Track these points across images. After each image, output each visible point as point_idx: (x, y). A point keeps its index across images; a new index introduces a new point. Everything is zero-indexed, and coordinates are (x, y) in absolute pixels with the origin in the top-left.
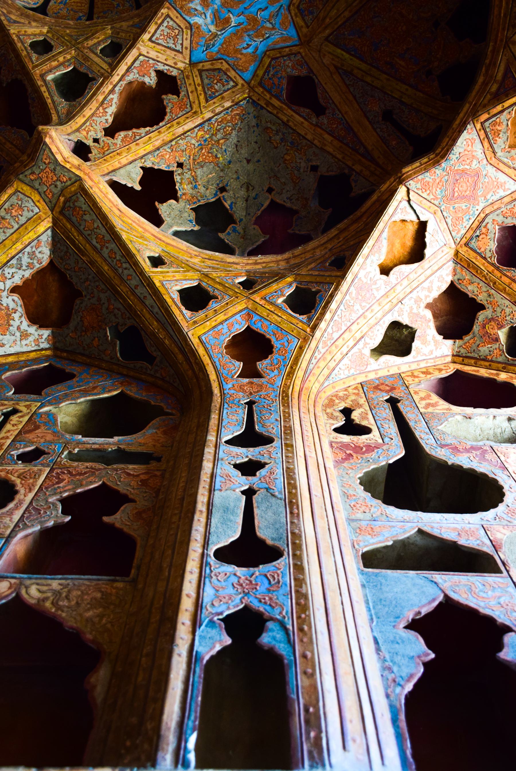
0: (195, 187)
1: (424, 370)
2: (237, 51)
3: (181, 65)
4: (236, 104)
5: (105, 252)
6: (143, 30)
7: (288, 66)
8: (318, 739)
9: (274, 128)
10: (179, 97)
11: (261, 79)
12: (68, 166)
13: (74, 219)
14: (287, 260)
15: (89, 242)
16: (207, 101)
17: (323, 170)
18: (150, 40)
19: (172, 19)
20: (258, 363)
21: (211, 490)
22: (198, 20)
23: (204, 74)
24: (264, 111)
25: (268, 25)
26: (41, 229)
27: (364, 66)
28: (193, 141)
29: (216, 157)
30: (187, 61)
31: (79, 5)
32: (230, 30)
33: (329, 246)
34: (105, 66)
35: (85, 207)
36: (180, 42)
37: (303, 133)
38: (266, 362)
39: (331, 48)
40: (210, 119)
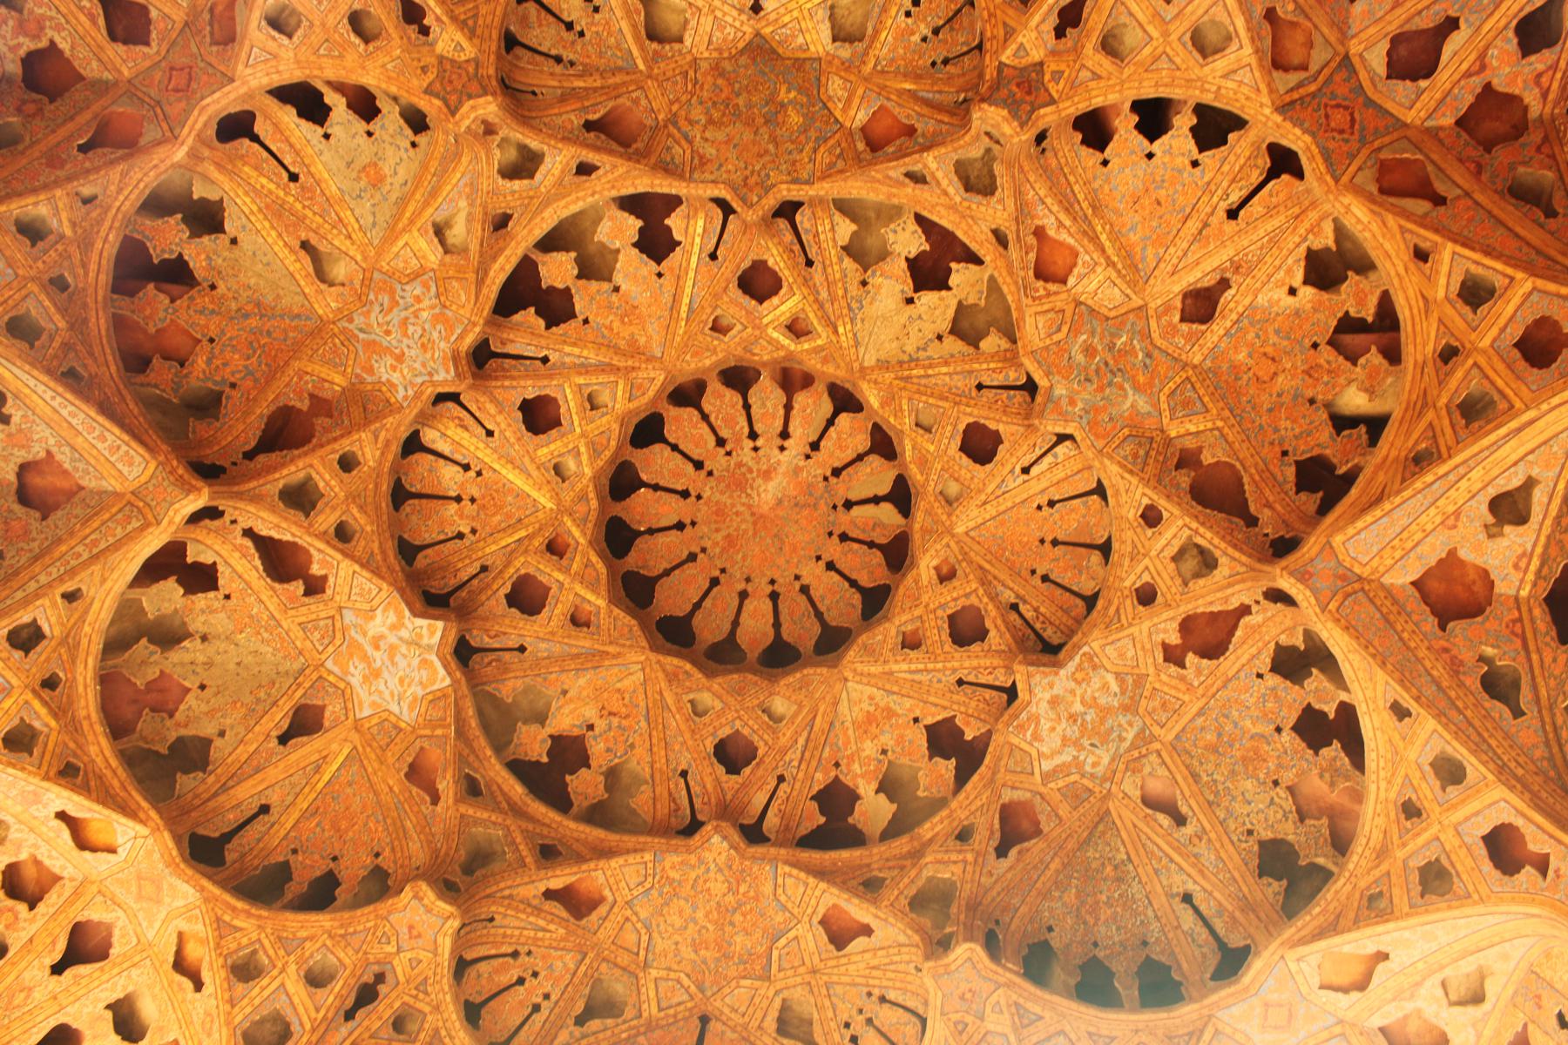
0: (203, 612)
2: (351, 656)
3: (337, 598)
5: (80, 549)
6: (362, 565)
12: (171, 513)
13: (120, 516)
14: (88, 717)
17: (218, 742)
26: (113, 482)
27: (320, 785)
32: (369, 650)
33: (99, 760)
34: (322, 529)
35: (130, 528)
39: (346, 751)
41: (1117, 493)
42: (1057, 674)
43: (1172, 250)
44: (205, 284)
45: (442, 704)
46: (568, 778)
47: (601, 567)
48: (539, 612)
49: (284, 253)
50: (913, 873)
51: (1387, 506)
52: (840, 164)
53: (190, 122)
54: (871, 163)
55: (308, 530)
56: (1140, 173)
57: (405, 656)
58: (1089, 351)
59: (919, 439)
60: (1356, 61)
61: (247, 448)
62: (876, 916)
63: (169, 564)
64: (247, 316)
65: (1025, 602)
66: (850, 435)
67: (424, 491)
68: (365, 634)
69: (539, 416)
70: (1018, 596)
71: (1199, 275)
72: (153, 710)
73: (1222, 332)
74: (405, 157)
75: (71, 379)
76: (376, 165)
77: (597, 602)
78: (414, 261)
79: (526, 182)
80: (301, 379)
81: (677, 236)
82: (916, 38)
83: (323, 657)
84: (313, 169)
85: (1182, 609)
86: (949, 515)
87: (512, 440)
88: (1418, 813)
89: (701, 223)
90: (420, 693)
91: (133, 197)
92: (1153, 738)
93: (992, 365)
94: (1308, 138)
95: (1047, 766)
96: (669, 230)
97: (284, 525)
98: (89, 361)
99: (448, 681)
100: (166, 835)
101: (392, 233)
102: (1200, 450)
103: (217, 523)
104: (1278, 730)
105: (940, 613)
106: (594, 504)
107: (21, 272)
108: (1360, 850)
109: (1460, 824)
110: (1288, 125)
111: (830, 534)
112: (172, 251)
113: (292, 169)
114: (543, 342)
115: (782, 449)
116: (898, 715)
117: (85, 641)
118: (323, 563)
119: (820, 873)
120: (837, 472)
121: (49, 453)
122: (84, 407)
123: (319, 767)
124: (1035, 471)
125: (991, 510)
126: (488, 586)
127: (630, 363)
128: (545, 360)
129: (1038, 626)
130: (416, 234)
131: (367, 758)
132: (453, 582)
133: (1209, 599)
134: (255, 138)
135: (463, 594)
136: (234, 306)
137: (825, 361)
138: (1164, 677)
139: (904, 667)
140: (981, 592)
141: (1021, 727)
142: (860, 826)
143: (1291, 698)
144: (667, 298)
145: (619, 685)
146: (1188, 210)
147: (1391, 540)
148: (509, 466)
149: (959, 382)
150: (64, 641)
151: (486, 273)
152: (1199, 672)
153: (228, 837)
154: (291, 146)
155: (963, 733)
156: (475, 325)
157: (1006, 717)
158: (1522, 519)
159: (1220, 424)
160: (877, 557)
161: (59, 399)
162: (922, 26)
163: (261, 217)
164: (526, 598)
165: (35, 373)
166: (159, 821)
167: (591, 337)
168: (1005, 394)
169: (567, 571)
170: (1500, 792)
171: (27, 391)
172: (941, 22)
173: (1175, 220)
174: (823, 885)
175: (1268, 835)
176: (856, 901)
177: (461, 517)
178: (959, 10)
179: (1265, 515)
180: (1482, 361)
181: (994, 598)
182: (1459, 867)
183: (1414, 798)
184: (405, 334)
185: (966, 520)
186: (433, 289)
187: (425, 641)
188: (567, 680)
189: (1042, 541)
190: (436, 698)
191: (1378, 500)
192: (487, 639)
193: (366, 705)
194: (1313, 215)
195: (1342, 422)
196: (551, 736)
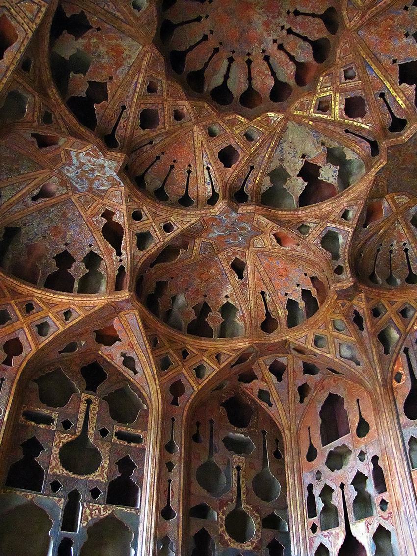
41: (183, 216)
42: (115, 171)
43: (263, 269)
50: (31, 89)
51: (143, 331)
52: (374, 189)
54: (366, 204)
56: (294, 279)
58: (243, 229)
59: (244, 128)
60: (287, 355)
62: (8, 68)
65: (151, 148)
66: (264, 83)
70: (155, 145)
71: (249, 271)
73: (225, 268)
81: (404, 85)
82: (395, 242)
85: (127, 230)
86: (204, 126)
88: (28, 312)
89: (400, 102)
92: (74, 193)
93: (258, 179)
94: (272, 342)
95: (73, 154)
102: (186, 248)
104: (67, 244)
105: (160, 107)
108: (15, 282)
109: (23, 330)
110: (280, 340)
111: (221, 44)
115: (275, 41)
116: (117, 69)
119: (37, 34)
120: (249, 62)
124: (206, 172)
125: (197, 145)
129: (138, 151)
133: (128, 243)
137: (302, 105)
138: (100, 206)
139: (140, 81)
140: (163, 131)
141: (94, 151)
142: (60, 37)
143: (80, 257)
144: (382, 57)
146: (273, 282)
147: (131, 326)
149: (259, 159)
152: (98, 222)
155: (98, 103)
157: (101, 144)
158: (124, 363)
159: (192, 258)
160: (199, 67)
162: (396, 247)
168: (244, 178)
170: (34, 351)
172: (392, 256)
173: (273, 276)
174: (30, 35)
175: (23, 231)
176: (18, 57)
178: (391, 268)
179: (153, 270)
180: (179, 368)
181: (158, 136)
182: (7, 327)
183: (34, 311)
185: (199, 134)
189: (175, 161)
191: (145, 326)
194: (248, 321)
195: (174, 298)
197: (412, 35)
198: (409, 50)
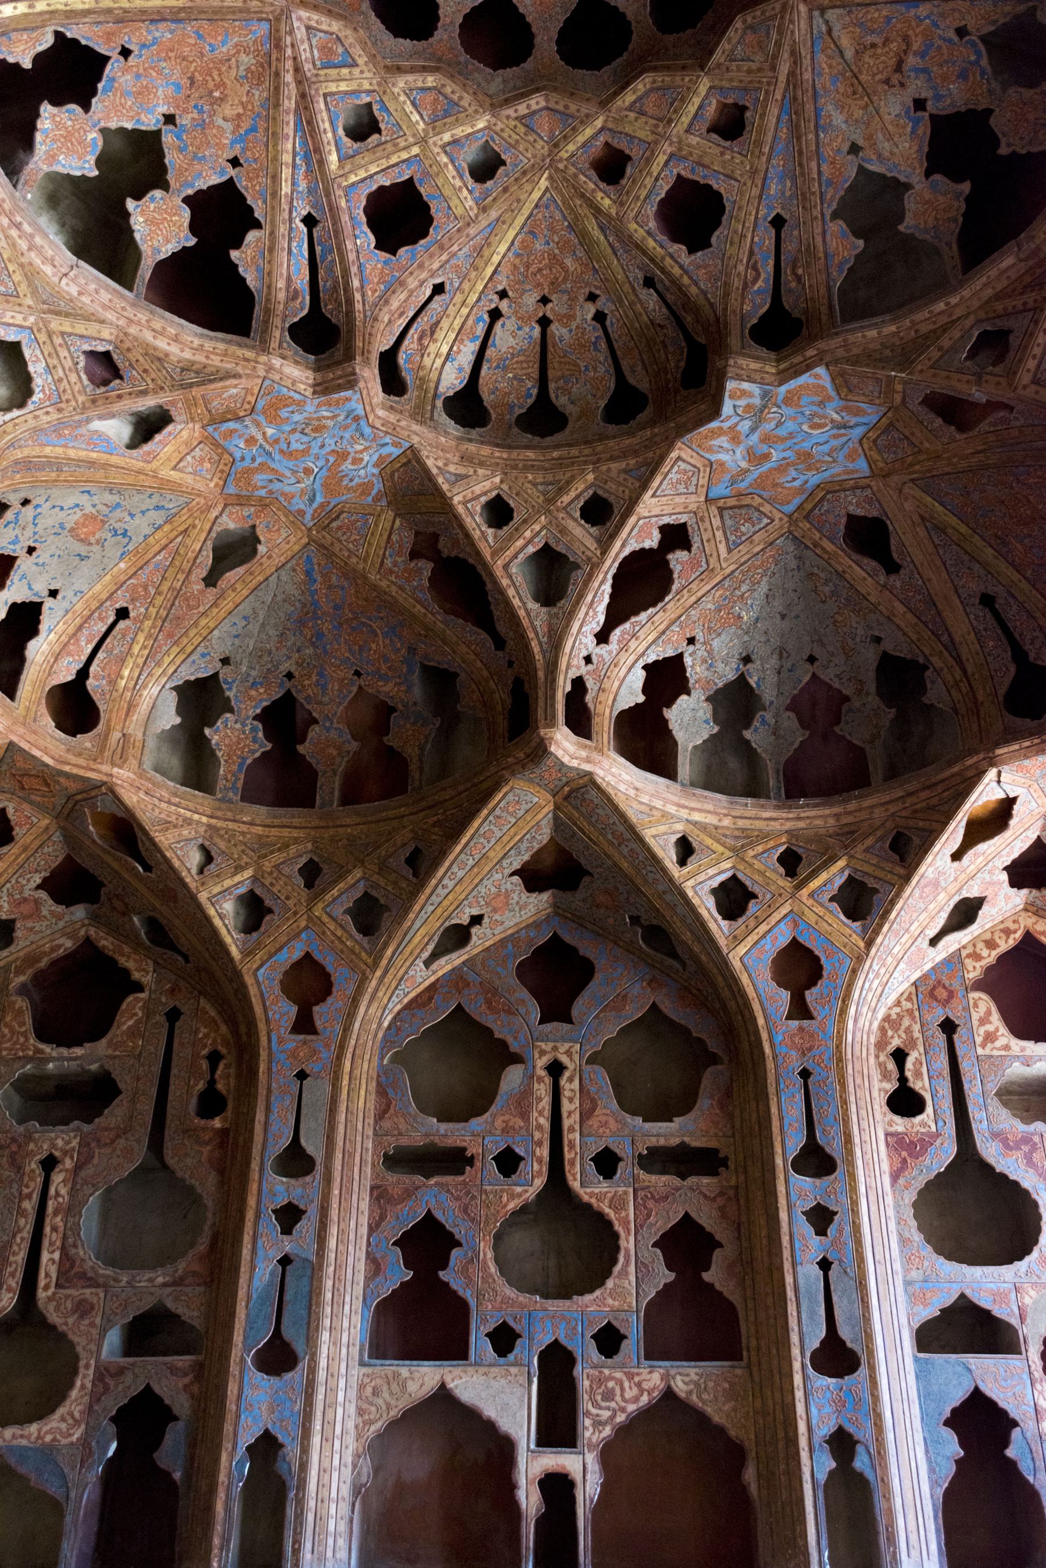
1: (988, 936)
3: (693, 507)
4: (771, 544)
6: (644, 486)
7: (850, 503)
8: (895, 1553)
9: (822, 575)
10: (689, 551)
11: (809, 514)
12: (575, 763)
13: (583, 810)
14: (837, 816)
15: (604, 837)
16: (730, 551)
17: (888, 646)
18: (653, 496)
19: (684, 461)
20: (807, 992)
21: (794, 1265)
22: (723, 457)
23: (726, 513)
24: (809, 553)
25: (827, 458)
26: (540, 816)
27: (963, 528)
28: (709, 606)
29: (740, 617)
30: (703, 499)
31: (525, 365)
32: (767, 466)
33: (892, 809)
34: (591, 544)
36: (694, 482)
37: (864, 592)
38: (815, 990)
39: (919, 494)
40: (733, 572)
44: (288, 685)
45: (855, 380)
46: (1003, 150)
47: (641, 85)
48: (718, 196)
49: (227, 605)
53: (81, 772)
55: (596, 566)
57: (779, 424)
61: (490, 643)
63: (644, 738)
64: (320, 635)
67: (536, 375)
68: (745, 472)
69: (400, 216)
72: (838, 721)
74: (49, 504)
75: (422, 863)
76: (72, 530)
77: (702, 97)
78: (197, 452)
79: (27, 353)
80: (391, 572)
81: (47, 41)
83: (778, 516)
84: (104, 596)
87: (444, 257)
90: (837, 403)
91: (191, 805)
96: (38, 58)
97: (589, 598)
98: (399, 840)
99: (821, 370)
100: (998, 752)
101: (165, 486)
103: (590, 684)
106: (536, 102)
107: (303, 924)
112: (254, 729)
113: (112, 619)
114: (283, 229)
117: (741, 823)
118: (640, 538)
121: (513, 874)
122: (452, 857)
123: (936, 527)
126: (674, 281)
127: (289, 78)
128: (310, 221)
130: (155, 464)
131: (929, 471)
132: (671, 331)
134: (83, 673)
135: (689, 319)
136: (309, 651)
144: (163, 33)
145: (849, 54)
148: (486, 253)
150: (737, 852)
151: (187, 368)
153: (1019, 654)
154: (80, 628)
156: (270, 368)
161: (445, 881)
163: (185, 640)
164: (693, 212)
165: (417, 908)
166: (981, 756)
167: (259, 151)
169: (651, 148)
171: (439, 911)
177: (571, 317)
184: (306, 452)
186: (231, 425)
187: (757, 401)
188: (833, 144)
190: (843, 385)
192: (760, 283)
193: (851, 466)
196: (928, 174)
197: (159, 131)
198: (129, 103)
